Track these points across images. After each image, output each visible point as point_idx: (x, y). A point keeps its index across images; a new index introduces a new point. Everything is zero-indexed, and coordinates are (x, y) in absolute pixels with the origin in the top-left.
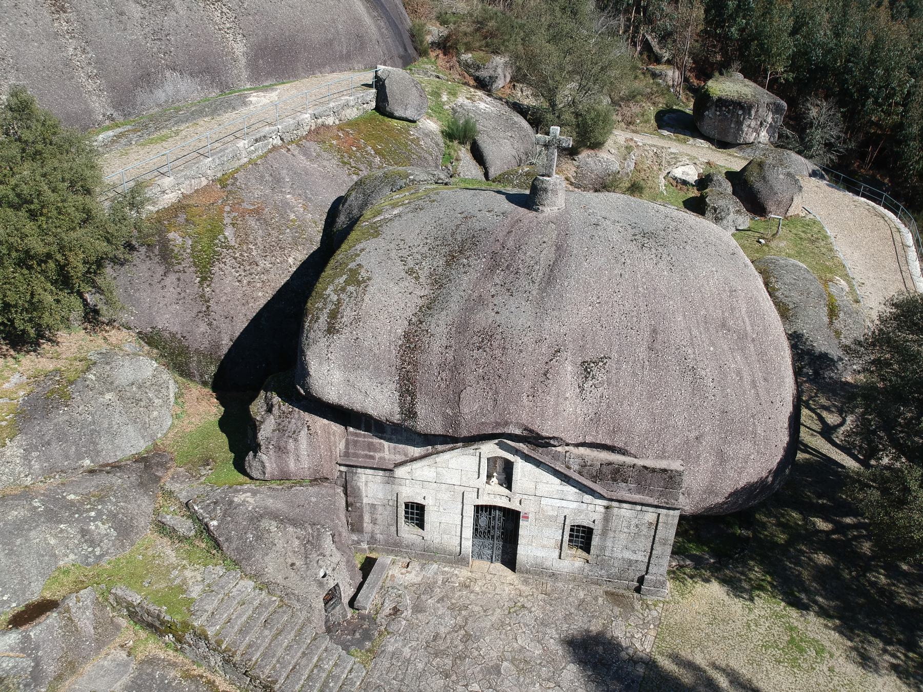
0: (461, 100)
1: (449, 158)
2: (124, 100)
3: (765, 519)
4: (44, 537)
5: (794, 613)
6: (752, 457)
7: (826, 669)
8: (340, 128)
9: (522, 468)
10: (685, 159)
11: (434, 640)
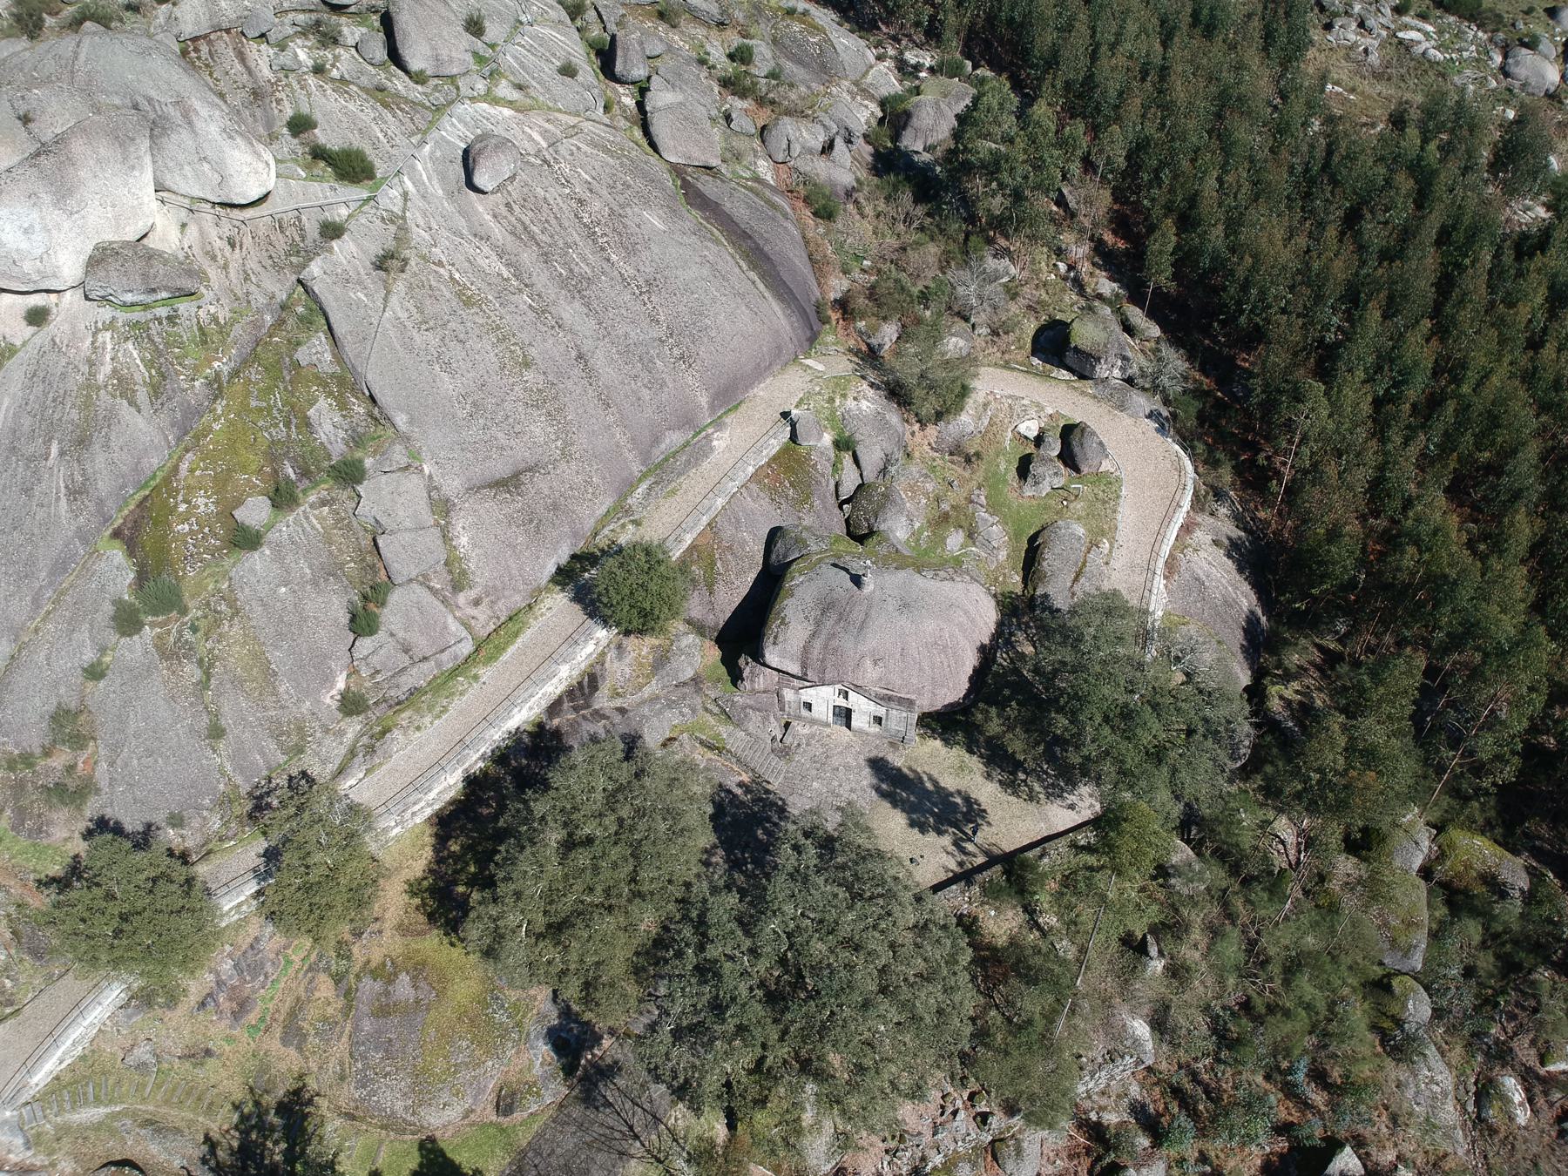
0: (850, 403)
1: (836, 466)
2: (645, 457)
4: (668, 714)
8: (768, 464)
9: (851, 693)
10: (1032, 412)
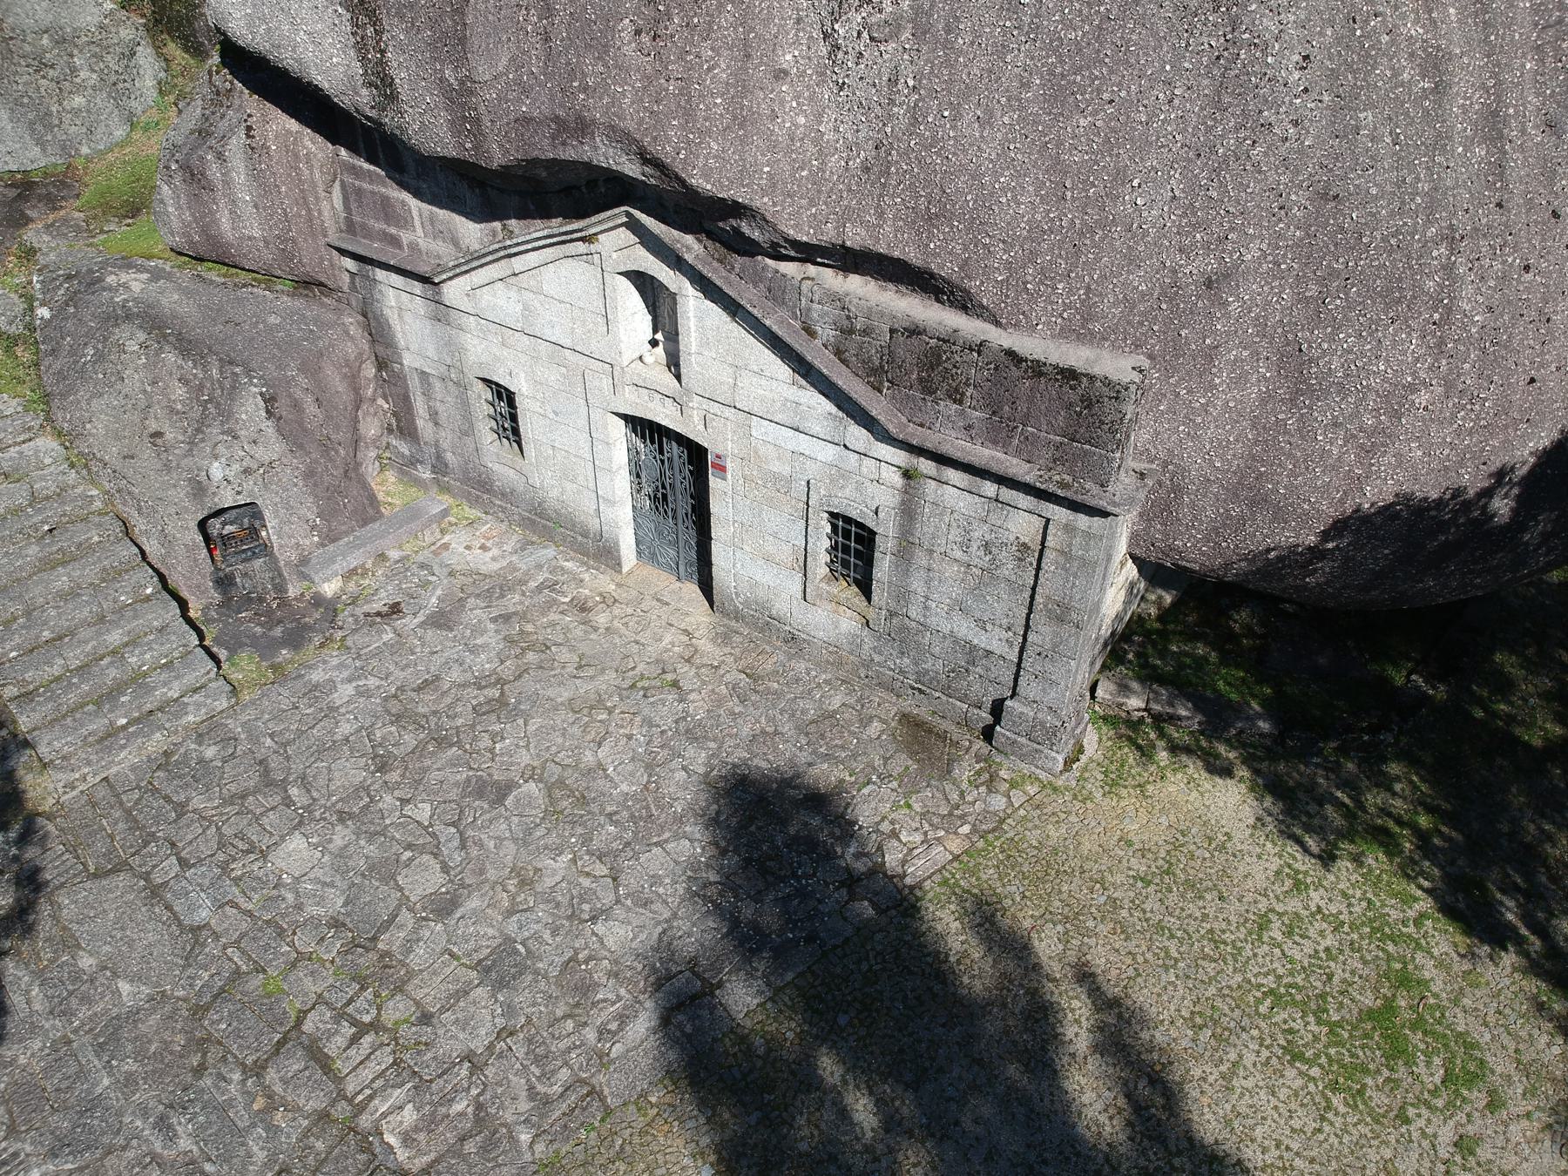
3: (1517, 673)
5: (1444, 939)
6: (1422, 398)
7: (1446, 1134)
11: (419, 689)
